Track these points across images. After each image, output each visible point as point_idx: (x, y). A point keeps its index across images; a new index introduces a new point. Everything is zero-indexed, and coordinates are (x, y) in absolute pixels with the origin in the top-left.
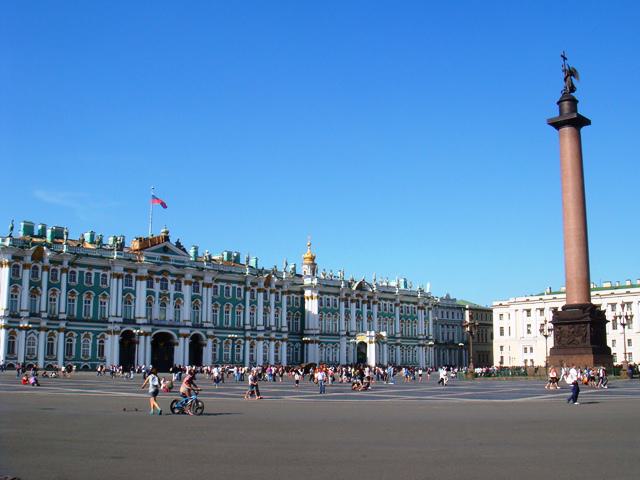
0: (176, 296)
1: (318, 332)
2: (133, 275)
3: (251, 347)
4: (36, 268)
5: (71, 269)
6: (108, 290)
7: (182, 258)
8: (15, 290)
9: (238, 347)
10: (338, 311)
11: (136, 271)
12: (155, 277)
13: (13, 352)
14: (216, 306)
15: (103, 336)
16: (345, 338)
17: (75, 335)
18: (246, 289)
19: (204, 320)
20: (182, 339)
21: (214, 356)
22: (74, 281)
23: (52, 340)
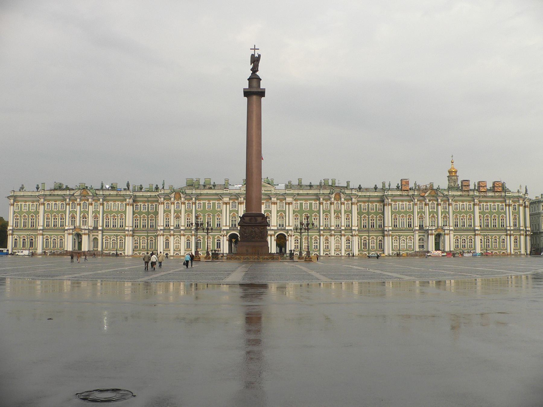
1: (390, 228)
3: (327, 239)
4: (178, 203)
5: (197, 202)
6: (221, 212)
7: (269, 189)
8: (167, 215)
10: (413, 212)
11: (238, 199)
14: (296, 216)
16: (417, 232)
17: (201, 237)
18: (320, 204)
19: (287, 224)
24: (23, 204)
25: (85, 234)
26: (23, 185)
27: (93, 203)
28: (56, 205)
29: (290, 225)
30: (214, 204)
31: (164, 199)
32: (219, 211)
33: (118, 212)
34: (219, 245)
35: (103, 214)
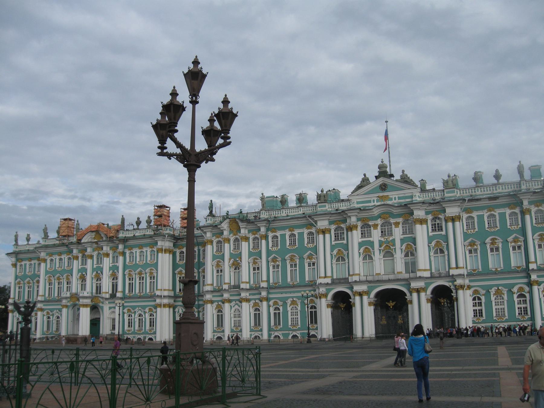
0: (402, 241)
2: (342, 226)
6: (315, 250)
7: (407, 192)
8: (218, 265)
9: (521, 296)
11: (345, 221)
12: (371, 223)
13: (222, 326)
14: (472, 244)
15: (312, 301)
17: (280, 303)
18: (523, 213)
19: (453, 265)
20: (415, 295)
21: (478, 314)
22: (277, 246)
23: (259, 310)
24: (28, 263)
25: (85, 306)
26: (28, 235)
27: (111, 252)
28: (59, 262)
29: (461, 264)
30: (301, 235)
31: (214, 235)
32: (310, 249)
33: (146, 265)
34: (314, 317)
35: (124, 270)
